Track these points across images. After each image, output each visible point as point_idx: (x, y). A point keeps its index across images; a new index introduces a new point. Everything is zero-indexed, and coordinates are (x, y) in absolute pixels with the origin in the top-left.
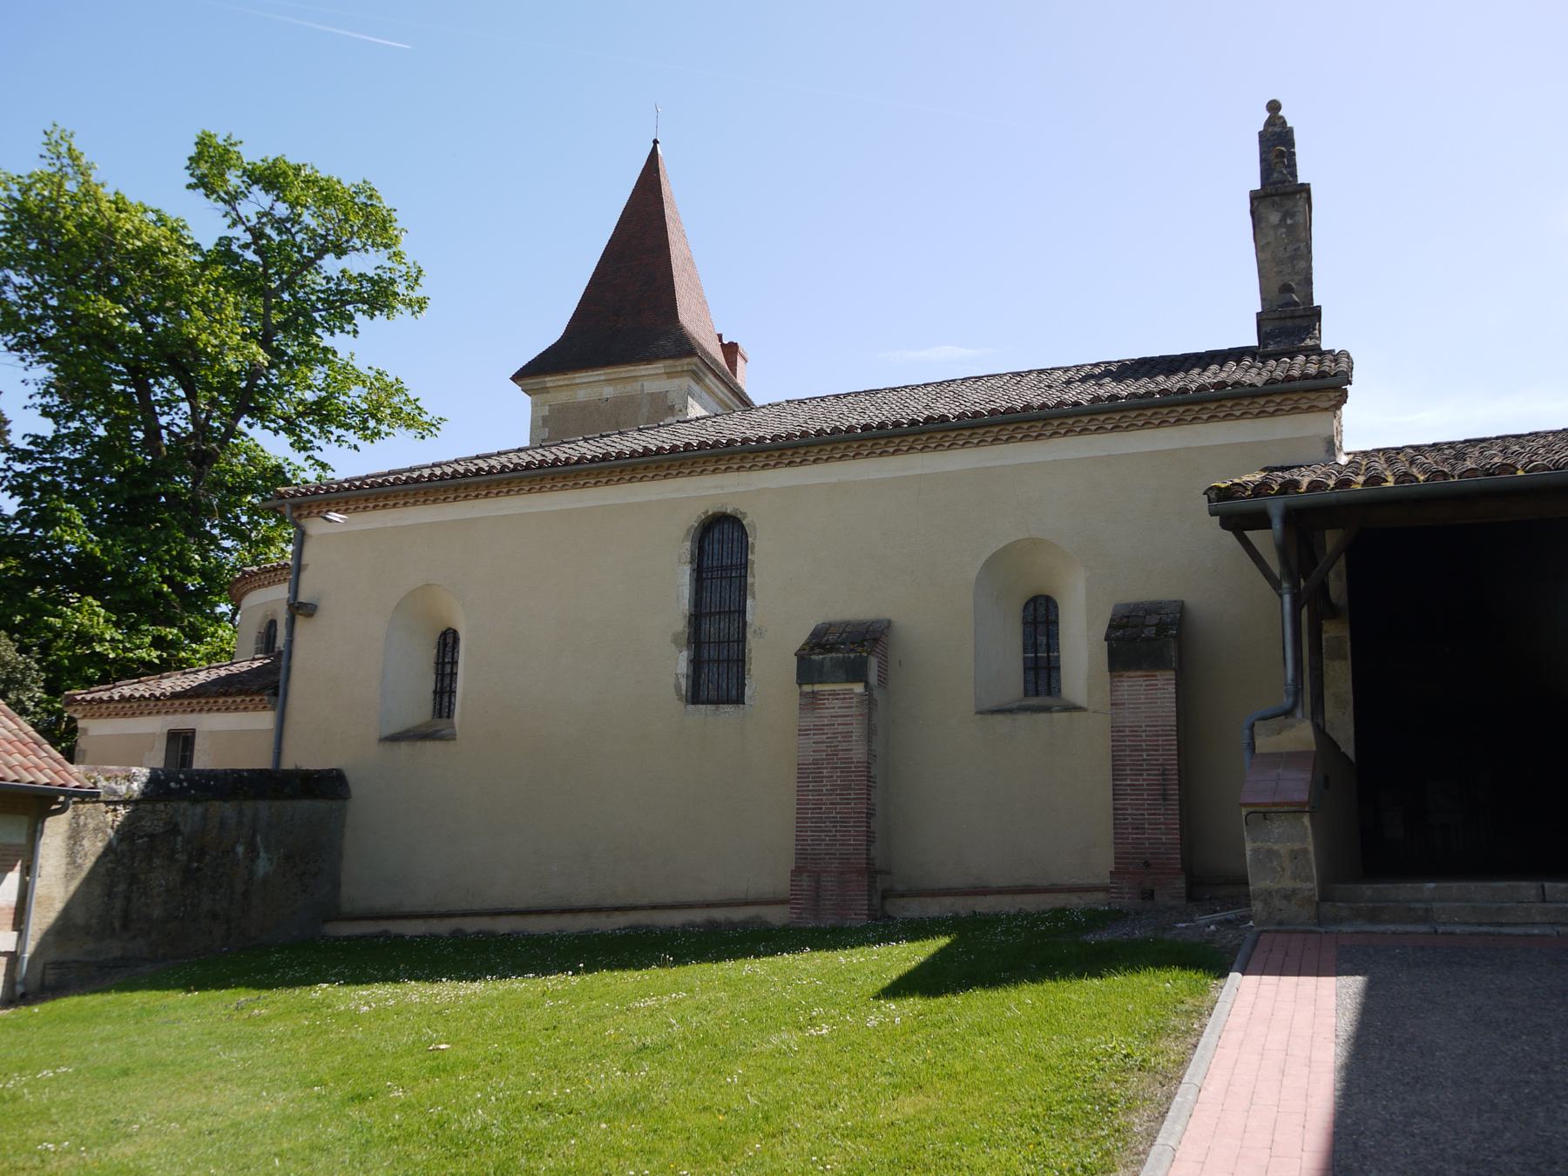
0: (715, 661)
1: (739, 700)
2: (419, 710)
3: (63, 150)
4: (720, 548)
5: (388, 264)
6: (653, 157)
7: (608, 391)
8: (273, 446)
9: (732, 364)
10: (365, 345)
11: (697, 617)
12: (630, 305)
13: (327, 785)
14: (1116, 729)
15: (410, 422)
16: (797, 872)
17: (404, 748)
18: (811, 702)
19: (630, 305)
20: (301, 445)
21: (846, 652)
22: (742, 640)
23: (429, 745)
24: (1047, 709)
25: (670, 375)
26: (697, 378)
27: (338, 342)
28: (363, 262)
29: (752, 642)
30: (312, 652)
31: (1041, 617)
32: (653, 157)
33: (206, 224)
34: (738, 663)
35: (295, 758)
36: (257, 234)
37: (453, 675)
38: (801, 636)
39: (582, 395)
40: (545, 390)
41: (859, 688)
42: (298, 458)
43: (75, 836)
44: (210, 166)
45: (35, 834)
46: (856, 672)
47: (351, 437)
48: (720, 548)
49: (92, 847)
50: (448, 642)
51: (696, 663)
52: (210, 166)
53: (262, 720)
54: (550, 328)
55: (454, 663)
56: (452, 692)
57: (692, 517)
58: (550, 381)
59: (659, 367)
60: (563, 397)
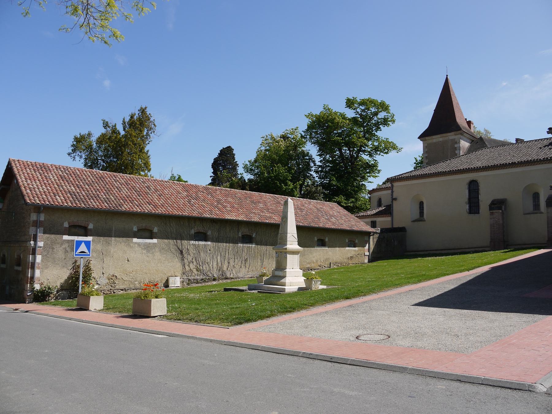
0: (474, 205)
1: (479, 213)
2: (417, 215)
3: (326, 108)
4: (473, 188)
5: (387, 114)
6: (447, 80)
7: (441, 139)
8: (365, 157)
9: (470, 126)
10: (384, 133)
11: (470, 199)
12: (444, 118)
13: (402, 230)
14: (548, 217)
15: (394, 149)
16: (491, 242)
17: (416, 223)
18: (492, 214)
19: (444, 118)
20: (371, 155)
21: (498, 205)
22: (478, 202)
23: (421, 222)
24: (536, 213)
25: (456, 135)
26: (462, 134)
27: (378, 133)
28: (382, 115)
29: (480, 203)
30: (396, 207)
31: (536, 196)
32: (447, 80)
33: (350, 114)
34: (478, 206)
35: (395, 226)
36: (361, 115)
37: (423, 210)
38: (489, 202)
39: (434, 141)
40: (426, 140)
41: (501, 211)
42: (370, 159)
43: (373, 239)
44: (350, 103)
45: (369, 238)
46: (500, 208)
47: (382, 154)
48: (473, 188)
49: (375, 240)
50: (421, 204)
51: (470, 207)
52: (350, 103)
53: (389, 219)
54: (425, 125)
55: (423, 207)
56: (423, 213)
57: (468, 181)
58: (427, 138)
59: (453, 133)
60: (430, 141)
